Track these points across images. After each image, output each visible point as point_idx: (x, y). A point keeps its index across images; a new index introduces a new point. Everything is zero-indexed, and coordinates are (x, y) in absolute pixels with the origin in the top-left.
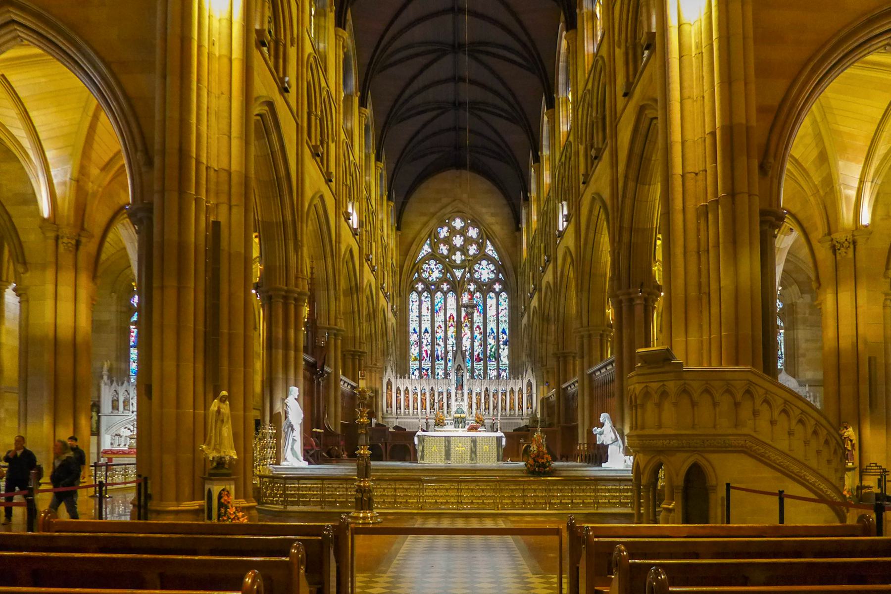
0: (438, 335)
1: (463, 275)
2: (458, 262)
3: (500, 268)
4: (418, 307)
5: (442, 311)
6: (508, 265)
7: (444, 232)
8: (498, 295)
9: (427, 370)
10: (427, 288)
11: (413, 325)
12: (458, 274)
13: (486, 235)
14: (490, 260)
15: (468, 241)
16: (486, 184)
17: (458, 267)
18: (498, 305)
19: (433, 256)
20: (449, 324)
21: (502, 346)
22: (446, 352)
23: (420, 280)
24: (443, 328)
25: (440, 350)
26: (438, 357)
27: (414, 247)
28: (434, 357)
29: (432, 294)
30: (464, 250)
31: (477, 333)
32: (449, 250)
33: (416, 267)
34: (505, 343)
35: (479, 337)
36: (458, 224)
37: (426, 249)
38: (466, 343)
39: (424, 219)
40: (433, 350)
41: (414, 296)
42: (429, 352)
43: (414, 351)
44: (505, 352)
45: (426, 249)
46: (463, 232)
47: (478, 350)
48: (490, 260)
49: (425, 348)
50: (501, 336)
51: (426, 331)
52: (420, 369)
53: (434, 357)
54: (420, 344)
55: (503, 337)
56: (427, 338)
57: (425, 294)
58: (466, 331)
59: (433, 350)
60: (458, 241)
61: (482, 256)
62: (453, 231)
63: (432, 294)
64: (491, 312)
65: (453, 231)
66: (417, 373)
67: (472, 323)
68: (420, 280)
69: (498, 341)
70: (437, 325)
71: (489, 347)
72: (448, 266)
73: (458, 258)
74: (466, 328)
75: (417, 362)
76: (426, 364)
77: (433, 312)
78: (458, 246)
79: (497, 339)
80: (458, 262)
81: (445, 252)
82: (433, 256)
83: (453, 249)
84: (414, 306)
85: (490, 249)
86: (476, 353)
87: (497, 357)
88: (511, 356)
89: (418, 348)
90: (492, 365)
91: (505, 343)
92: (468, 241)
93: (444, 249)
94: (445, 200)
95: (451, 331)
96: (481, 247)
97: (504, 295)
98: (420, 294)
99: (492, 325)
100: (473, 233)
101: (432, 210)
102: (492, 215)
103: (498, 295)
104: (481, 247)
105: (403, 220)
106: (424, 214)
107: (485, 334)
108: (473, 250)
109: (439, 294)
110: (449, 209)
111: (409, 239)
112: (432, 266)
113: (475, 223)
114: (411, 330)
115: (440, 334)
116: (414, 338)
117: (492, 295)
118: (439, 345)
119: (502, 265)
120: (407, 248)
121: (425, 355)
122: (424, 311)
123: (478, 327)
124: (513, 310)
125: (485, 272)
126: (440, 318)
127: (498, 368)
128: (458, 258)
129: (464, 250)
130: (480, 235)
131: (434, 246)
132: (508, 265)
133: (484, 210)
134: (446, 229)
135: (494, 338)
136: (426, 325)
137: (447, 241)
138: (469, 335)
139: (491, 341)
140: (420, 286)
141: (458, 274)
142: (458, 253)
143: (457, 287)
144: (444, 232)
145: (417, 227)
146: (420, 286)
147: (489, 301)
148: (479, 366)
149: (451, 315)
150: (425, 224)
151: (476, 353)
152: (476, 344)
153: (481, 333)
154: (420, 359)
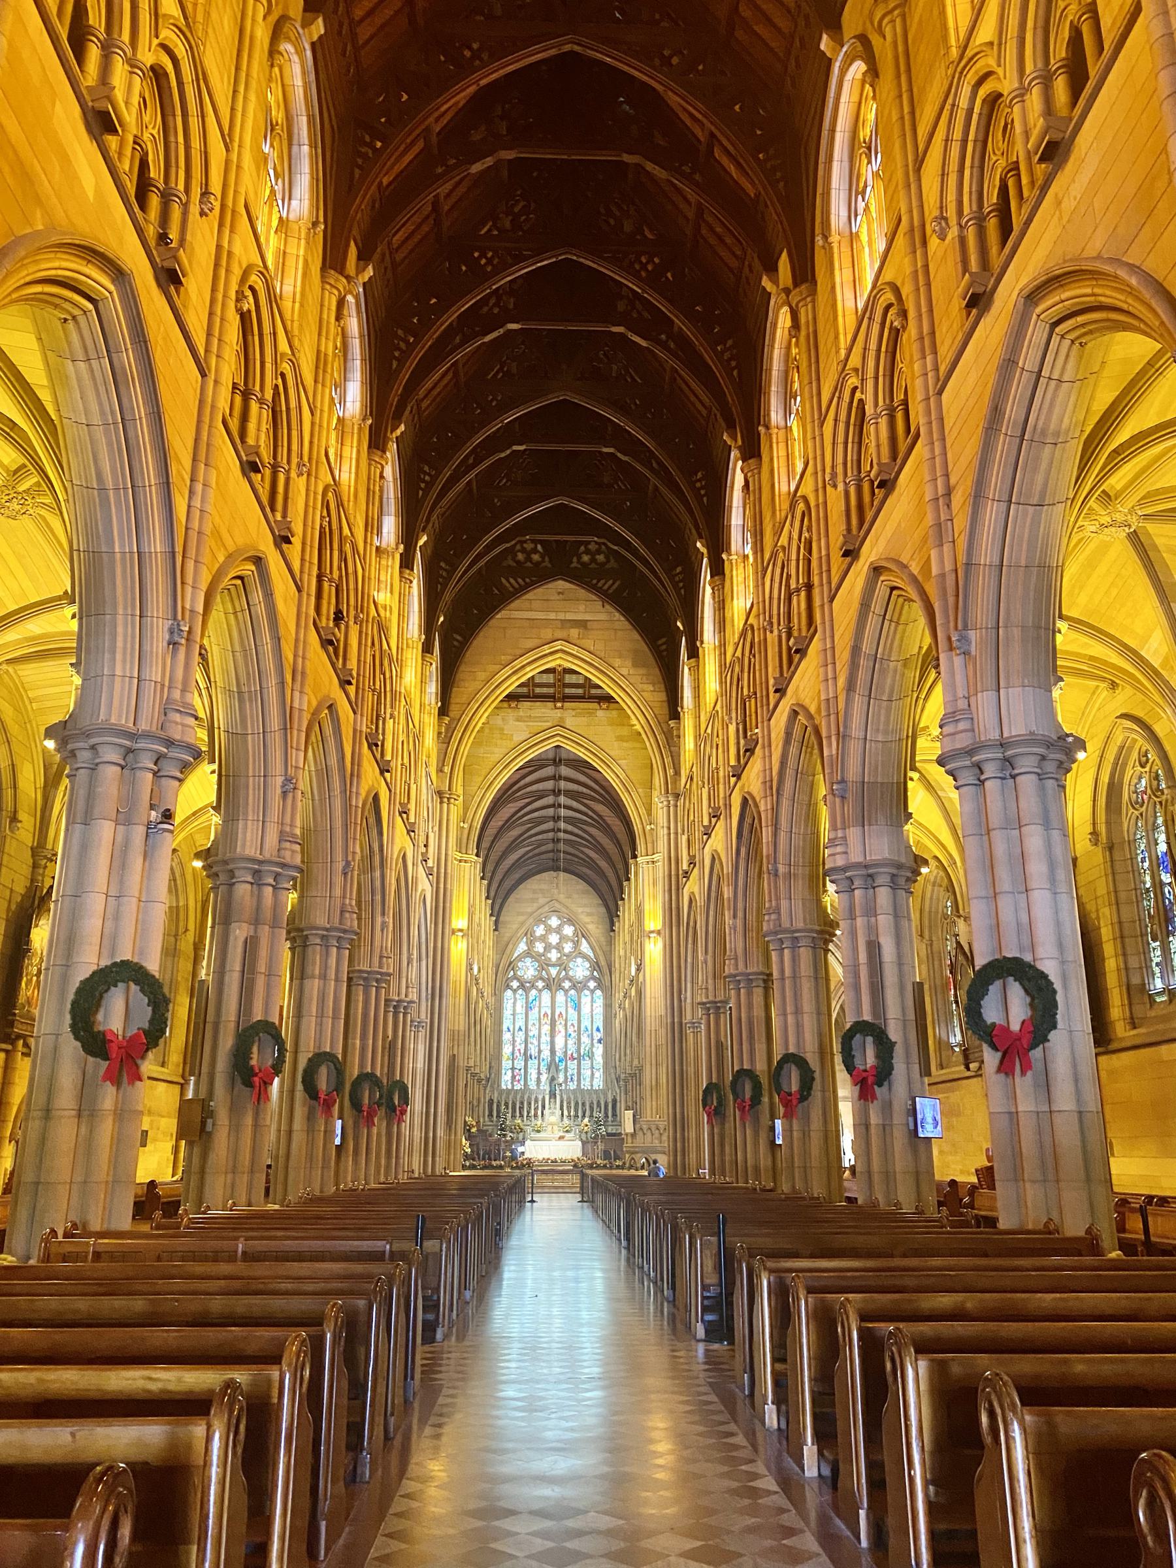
0: (531, 1034)
1: (559, 973)
2: (554, 959)
3: (595, 966)
4: (512, 1004)
6: (603, 963)
7: (540, 931)
8: (592, 992)
10: (522, 986)
11: (507, 1023)
12: (554, 971)
13: (581, 933)
14: (585, 957)
15: (563, 938)
16: (582, 885)
17: (554, 965)
18: (592, 1001)
19: (528, 954)
20: (543, 1022)
21: (596, 1045)
22: (540, 1051)
23: (515, 977)
25: (533, 1051)
27: (510, 946)
28: (527, 1057)
29: (527, 991)
30: (559, 948)
31: (571, 1030)
32: (545, 948)
33: (511, 965)
34: (599, 1041)
36: (554, 922)
37: (522, 947)
39: (521, 918)
41: (509, 993)
44: (599, 1050)
45: (522, 947)
46: (558, 930)
47: (572, 1049)
48: (585, 957)
49: (518, 1047)
51: (520, 1029)
52: (513, 1069)
53: (527, 1057)
55: (598, 1036)
56: (520, 1037)
57: (520, 991)
58: (560, 1027)
60: (554, 939)
62: (549, 930)
63: (527, 991)
64: (586, 1009)
65: (549, 930)
66: (509, 1073)
67: (566, 1020)
68: (515, 977)
69: (592, 1040)
70: (530, 1023)
72: (544, 964)
73: (554, 955)
76: (520, 1064)
77: (528, 1008)
78: (554, 944)
80: (554, 959)
81: (541, 950)
82: (528, 954)
83: (548, 948)
85: (585, 947)
86: (569, 1053)
87: (591, 1056)
88: (606, 1054)
90: (586, 1063)
91: (599, 1041)
92: (563, 938)
93: (539, 947)
94: (542, 901)
95: (546, 1029)
96: (577, 944)
97: (598, 993)
98: (515, 991)
99: (586, 1023)
100: (568, 930)
101: (529, 910)
102: (589, 914)
103: (592, 992)
104: (577, 944)
105: (501, 918)
106: (522, 914)
108: (568, 947)
109: (534, 992)
110: (546, 908)
111: (506, 939)
113: (571, 922)
114: (505, 1028)
115: (533, 1031)
117: (587, 992)
119: (597, 963)
120: (503, 948)
124: (608, 1006)
125: (580, 969)
127: (592, 1068)
128: (554, 955)
129: (559, 948)
130: (576, 934)
131: (530, 944)
132: (603, 963)
133: (580, 910)
134: (542, 927)
136: (520, 1023)
137: (543, 938)
138: (563, 1033)
139: (585, 1039)
140: (515, 984)
141: (554, 971)
142: (554, 951)
143: (552, 985)
144: (540, 931)
145: (515, 926)
146: (515, 984)
148: (572, 1065)
150: (522, 923)
152: (571, 1042)
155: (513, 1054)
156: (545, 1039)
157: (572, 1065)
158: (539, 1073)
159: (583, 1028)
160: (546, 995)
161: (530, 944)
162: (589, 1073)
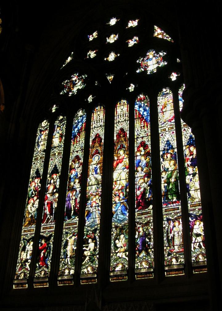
5: (83, 134)
9: (47, 239)
11: (37, 165)
21: (190, 170)
22: (84, 199)
24: (82, 161)
26: (69, 210)
35: (144, 161)
38: (120, 175)
40: (62, 200)
42: (55, 205)
43: (32, 207)
47: (142, 183)
50: (187, 152)
51: (55, 171)
52: (37, 238)
54: (41, 194)
59: (62, 200)
61: (149, 44)
66: (30, 247)
67: (132, 139)
70: (72, 156)
71: (164, 176)
74: (121, 152)
75: (33, 227)
77: (68, 138)
79: (180, 158)
84: (42, 138)
86: (138, 193)
87: (182, 192)
89: (37, 202)
90: (170, 210)
95: (95, 161)
107: (155, 156)
112: (74, 79)
114: (32, 172)
115: (77, 170)
116: (35, 184)
118: (73, 189)
121: (47, 211)
122: (56, 141)
123: (143, 144)
126: (77, 148)
127: (185, 216)
135: (173, 157)
136: (56, 161)
138: (126, 161)
139: (168, 164)
147: (161, 101)
149: (97, 136)
151: (138, 193)
152: (140, 174)
153: (146, 155)
154: (39, 219)
155: (40, 209)
156: (94, 178)
157: (144, 217)
158: (81, 242)
159: (162, 146)
160: (99, 115)
161: (81, 55)
162: (178, 228)
